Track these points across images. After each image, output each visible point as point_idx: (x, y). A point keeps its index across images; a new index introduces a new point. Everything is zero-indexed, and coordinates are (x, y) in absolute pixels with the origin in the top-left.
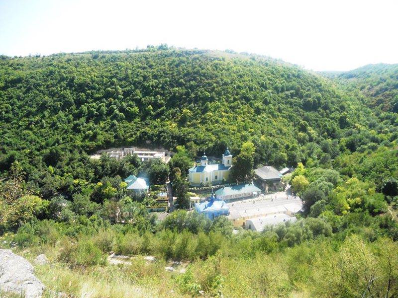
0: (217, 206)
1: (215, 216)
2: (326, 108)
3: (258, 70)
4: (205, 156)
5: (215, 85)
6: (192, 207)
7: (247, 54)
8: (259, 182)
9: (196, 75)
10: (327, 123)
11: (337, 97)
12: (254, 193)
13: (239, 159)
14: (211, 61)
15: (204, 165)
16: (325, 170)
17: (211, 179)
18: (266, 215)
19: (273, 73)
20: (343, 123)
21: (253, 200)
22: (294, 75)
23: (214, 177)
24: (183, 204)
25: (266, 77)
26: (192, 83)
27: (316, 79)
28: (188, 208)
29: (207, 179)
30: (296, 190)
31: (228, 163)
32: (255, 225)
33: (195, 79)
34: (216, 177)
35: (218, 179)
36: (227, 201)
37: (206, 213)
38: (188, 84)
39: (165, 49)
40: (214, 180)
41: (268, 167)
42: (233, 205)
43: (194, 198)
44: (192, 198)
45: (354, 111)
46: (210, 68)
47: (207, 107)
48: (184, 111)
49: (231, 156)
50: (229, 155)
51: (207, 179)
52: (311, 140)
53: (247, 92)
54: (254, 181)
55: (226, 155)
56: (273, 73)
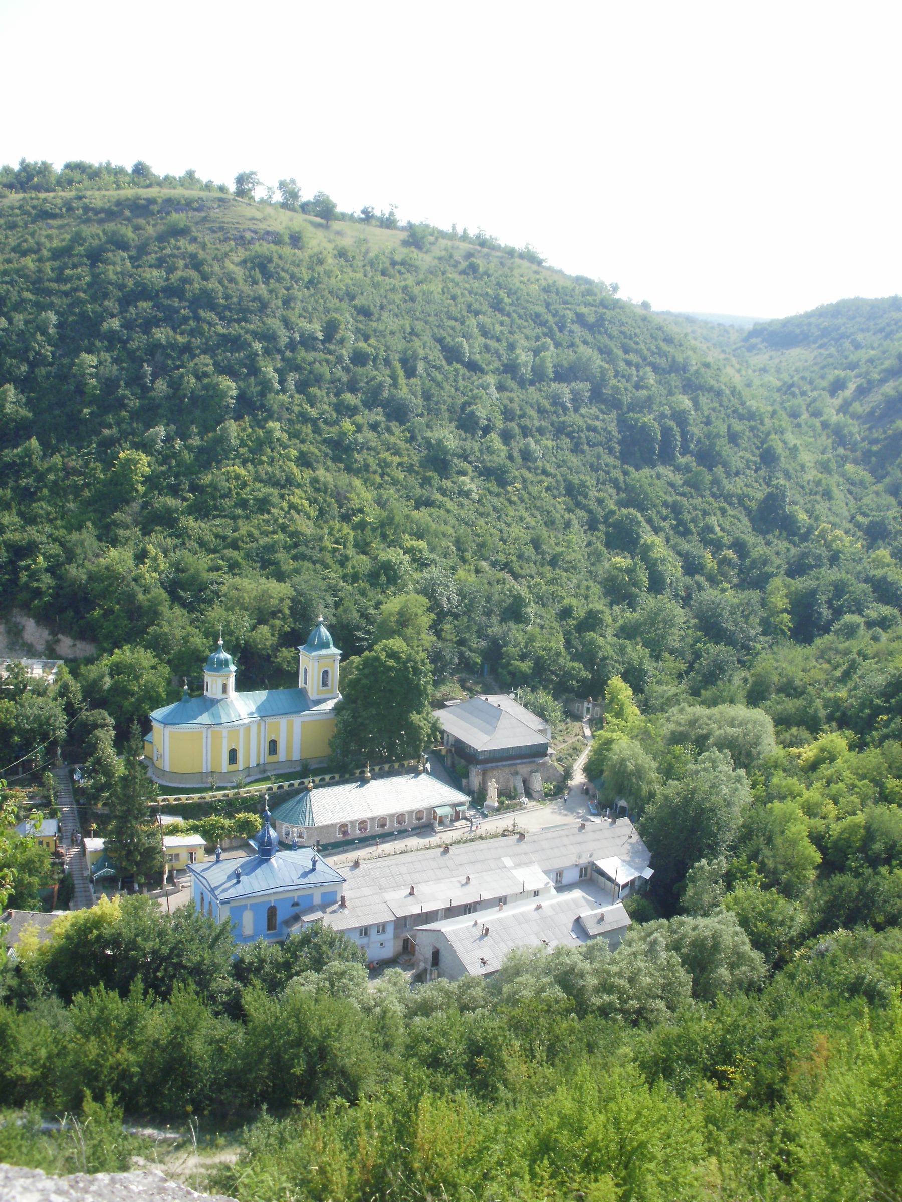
0: (287, 869)
1: (280, 917)
2: (707, 457)
3: (435, 287)
4: (225, 655)
5: (257, 346)
6: (171, 879)
7: (388, 223)
8: (457, 764)
9: (176, 303)
10: (713, 520)
11: (751, 416)
12: (440, 812)
13: (373, 667)
14: (241, 241)
15: (219, 695)
16: (715, 710)
17: (252, 754)
18: (501, 901)
19: (497, 305)
20: (770, 517)
21: (434, 840)
22: (580, 319)
23: (264, 747)
24: (136, 869)
25: (472, 321)
26: (161, 334)
27: (669, 340)
28: (154, 880)
29: (233, 756)
30: (611, 791)
31: (324, 684)
32: (459, 948)
33: (171, 319)
34: (273, 746)
35: (282, 755)
36: (328, 848)
37: (237, 906)
38: (138, 341)
39: (37, 188)
40: (265, 758)
41: (493, 699)
42: (356, 865)
43: (180, 841)
44: (169, 841)
45: (811, 475)
46: (239, 273)
47: (221, 440)
48: (122, 455)
49: (334, 650)
50: (326, 645)
51: (233, 756)
52: (657, 585)
53: (394, 377)
54: (436, 756)
55: (313, 647)
56: (497, 305)
